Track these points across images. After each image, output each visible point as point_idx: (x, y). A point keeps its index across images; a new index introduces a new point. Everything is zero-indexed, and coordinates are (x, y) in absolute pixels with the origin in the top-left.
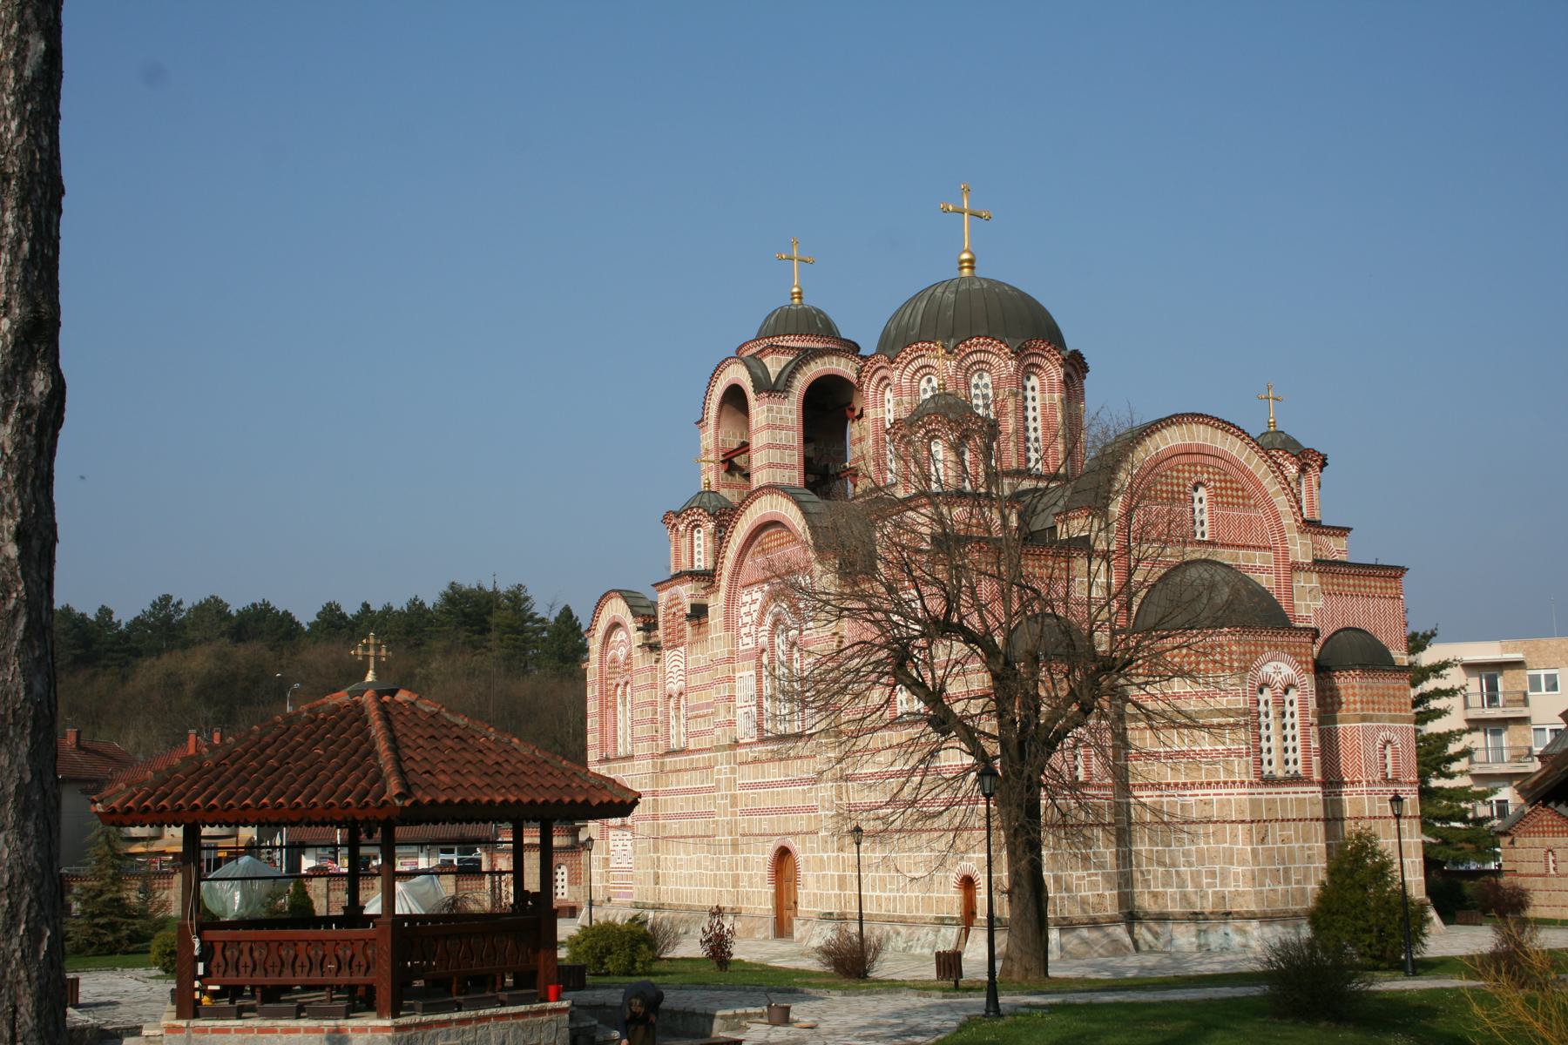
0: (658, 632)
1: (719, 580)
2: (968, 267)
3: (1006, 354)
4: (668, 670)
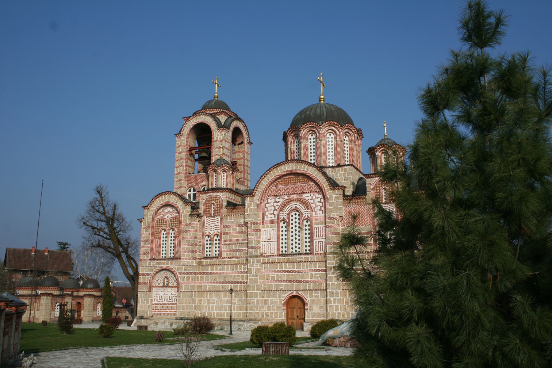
0: (199, 210)
1: (256, 193)
2: (323, 100)
3: (355, 131)
4: (206, 225)
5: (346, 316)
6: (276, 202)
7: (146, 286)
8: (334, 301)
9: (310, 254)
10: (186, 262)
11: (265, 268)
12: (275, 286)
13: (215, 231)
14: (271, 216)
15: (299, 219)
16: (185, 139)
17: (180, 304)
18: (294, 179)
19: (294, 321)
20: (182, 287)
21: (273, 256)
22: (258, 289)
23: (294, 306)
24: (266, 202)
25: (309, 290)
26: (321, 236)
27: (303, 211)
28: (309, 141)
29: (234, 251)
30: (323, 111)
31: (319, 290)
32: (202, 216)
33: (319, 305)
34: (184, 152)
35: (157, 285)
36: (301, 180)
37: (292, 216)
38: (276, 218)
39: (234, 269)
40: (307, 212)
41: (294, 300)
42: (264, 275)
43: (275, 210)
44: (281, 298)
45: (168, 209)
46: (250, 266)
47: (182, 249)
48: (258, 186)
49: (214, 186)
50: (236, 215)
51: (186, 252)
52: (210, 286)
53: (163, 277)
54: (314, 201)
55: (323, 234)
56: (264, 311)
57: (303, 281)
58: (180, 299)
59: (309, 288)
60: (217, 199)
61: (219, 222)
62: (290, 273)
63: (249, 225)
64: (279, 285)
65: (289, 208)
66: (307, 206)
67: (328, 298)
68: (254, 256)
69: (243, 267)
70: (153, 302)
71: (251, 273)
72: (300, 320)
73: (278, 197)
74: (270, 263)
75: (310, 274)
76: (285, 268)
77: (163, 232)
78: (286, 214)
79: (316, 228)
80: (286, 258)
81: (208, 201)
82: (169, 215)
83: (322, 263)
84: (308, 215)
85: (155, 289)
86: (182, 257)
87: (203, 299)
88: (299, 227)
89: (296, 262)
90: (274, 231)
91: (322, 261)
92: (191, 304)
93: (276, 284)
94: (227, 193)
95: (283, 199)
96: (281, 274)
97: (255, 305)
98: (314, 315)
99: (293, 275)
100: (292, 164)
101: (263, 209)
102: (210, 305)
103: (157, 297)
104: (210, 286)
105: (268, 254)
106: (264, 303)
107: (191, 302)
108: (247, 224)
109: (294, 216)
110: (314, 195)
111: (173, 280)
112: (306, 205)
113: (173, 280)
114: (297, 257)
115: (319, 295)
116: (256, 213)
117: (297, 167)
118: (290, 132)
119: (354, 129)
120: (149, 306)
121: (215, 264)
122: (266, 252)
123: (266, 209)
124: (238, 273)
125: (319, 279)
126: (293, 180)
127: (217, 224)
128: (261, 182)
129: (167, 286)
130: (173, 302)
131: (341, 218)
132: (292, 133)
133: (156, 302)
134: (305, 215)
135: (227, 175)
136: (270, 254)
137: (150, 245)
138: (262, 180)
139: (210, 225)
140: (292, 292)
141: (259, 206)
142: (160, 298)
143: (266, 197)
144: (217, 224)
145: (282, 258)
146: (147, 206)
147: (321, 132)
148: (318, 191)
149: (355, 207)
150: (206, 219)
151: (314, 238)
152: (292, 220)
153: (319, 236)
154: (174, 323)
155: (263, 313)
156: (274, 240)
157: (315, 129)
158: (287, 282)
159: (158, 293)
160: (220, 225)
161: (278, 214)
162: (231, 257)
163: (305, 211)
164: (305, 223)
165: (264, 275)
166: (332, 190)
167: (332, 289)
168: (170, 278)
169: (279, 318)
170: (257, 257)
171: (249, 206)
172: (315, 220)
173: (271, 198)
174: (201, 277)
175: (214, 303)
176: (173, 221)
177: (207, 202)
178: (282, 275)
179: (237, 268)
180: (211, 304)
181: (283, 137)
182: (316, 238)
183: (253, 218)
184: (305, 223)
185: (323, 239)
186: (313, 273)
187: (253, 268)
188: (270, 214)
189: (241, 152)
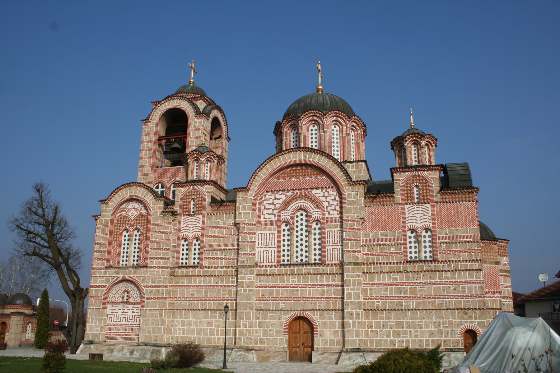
0: (174, 207)
1: (250, 186)
3: (362, 126)
4: (182, 226)
5: (369, 344)
6: (276, 199)
7: (99, 302)
8: (353, 325)
9: (321, 264)
10: (155, 271)
11: (260, 282)
12: (273, 305)
13: (195, 233)
14: (270, 216)
15: (306, 221)
16: (154, 126)
17: (144, 326)
18: (301, 171)
19: (298, 349)
20: (148, 303)
21: (272, 266)
22: (251, 308)
23: (298, 330)
24: (263, 199)
25: (319, 310)
26: (336, 242)
27: (312, 211)
28: (310, 132)
29: (220, 258)
30: (326, 99)
31: (332, 310)
32: (177, 215)
33: (332, 330)
34: (152, 141)
35: (113, 301)
36: (310, 173)
37: (297, 217)
38: (276, 219)
39: (218, 282)
41: (298, 322)
42: (260, 290)
43: (275, 208)
44: (281, 320)
45: (133, 204)
46: (241, 278)
47: (150, 254)
48: (254, 178)
49: (195, 178)
50: (223, 214)
51: (155, 258)
52: (186, 303)
53: (123, 290)
54: (326, 199)
55: (338, 239)
56: (259, 336)
57: (312, 299)
58: (145, 319)
59: (319, 308)
60: (198, 193)
61: (201, 222)
62: (294, 289)
63: (241, 227)
64: (279, 303)
65: (294, 207)
66: (318, 204)
67: (346, 320)
68: (246, 266)
69: (231, 279)
70: (107, 323)
71: (243, 287)
72: (305, 349)
73: (280, 193)
74: (267, 275)
75: (321, 289)
76: (288, 281)
77: (125, 233)
78: (289, 214)
79: (328, 232)
80: (289, 268)
81: (186, 196)
82: (134, 212)
83: (337, 275)
84: (319, 216)
85: (111, 305)
86: (149, 266)
87: (176, 320)
88: (306, 231)
89: (302, 274)
90: (274, 234)
91: (337, 274)
92: (160, 326)
93: (275, 301)
94: (212, 186)
95: (286, 195)
96: (281, 290)
97: (248, 328)
98: (326, 341)
99: (298, 290)
100: (300, 153)
101: (260, 207)
102: (186, 327)
103: (113, 316)
104: (186, 303)
105: (265, 264)
106: (258, 326)
107: (160, 323)
108: (238, 226)
109: (300, 217)
110: (326, 191)
111: (135, 294)
112: (315, 203)
113: (135, 294)
114: (304, 268)
115: (333, 316)
116: (250, 212)
117: (305, 157)
118: (285, 122)
119: (360, 124)
120: (101, 327)
121: (194, 275)
122: (262, 261)
123: (263, 208)
124: (225, 287)
125: (333, 296)
126: (299, 173)
127: (198, 225)
128: (257, 173)
129: (128, 302)
130: (135, 323)
131: (362, 220)
132: (288, 123)
133: (111, 323)
134: (314, 216)
135: (211, 166)
136: (267, 264)
137: (106, 249)
138: (259, 171)
140: (296, 312)
141: (254, 203)
142: (117, 318)
143: (263, 192)
144: (198, 225)
145: (283, 268)
146: (106, 200)
147: (325, 122)
148: (332, 187)
149: (380, 207)
150: (183, 218)
151: (327, 244)
152: (297, 221)
153: (333, 242)
154: (135, 351)
155: (257, 339)
157: (318, 119)
158: (289, 299)
159: (114, 311)
162: (215, 267)
163: (315, 210)
164: (314, 225)
165: (260, 290)
166: (350, 185)
167: (351, 309)
168: (131, 292)
169: (278, 346)
170: (251, 266)
171: (242, 202)
172: (328, 222)
173: (269, 194)
174: (174, 291)
175: (190, 325)
176: (139, 220)
177: (185, 197)
178: (283, 290)
179: (222, 280)
180: (186, 326)
181: (274, 129)
182: (329, 244)
183: (247, 217)
184: (314, 225)
185: (338, 246)
186: (325, 289)
187: (245, 281)
188: (269, 214)
189: (219, 147)
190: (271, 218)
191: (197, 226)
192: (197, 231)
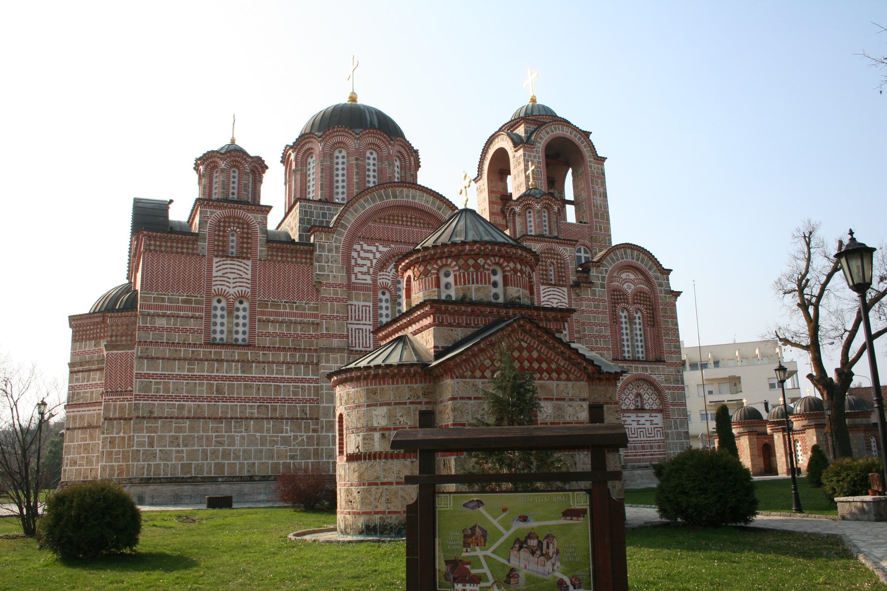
4: (214, 274)
13: (240, 289)
40: (383, 277)
61: (249, 272)
105: (357, 348)
123: (353, 262)
136: (361, 349)
139: (226, 275)
156: (368, 322)
160: (249, 277)
161: (375, 273)
188: (362, 273)
190: (366, 280)
191: (243, 278)
192: (243, 286)
